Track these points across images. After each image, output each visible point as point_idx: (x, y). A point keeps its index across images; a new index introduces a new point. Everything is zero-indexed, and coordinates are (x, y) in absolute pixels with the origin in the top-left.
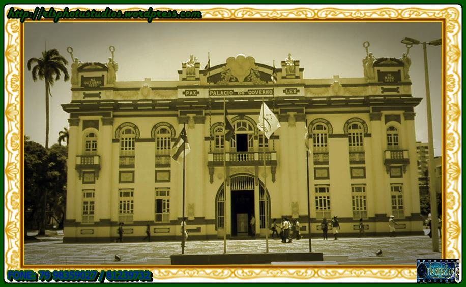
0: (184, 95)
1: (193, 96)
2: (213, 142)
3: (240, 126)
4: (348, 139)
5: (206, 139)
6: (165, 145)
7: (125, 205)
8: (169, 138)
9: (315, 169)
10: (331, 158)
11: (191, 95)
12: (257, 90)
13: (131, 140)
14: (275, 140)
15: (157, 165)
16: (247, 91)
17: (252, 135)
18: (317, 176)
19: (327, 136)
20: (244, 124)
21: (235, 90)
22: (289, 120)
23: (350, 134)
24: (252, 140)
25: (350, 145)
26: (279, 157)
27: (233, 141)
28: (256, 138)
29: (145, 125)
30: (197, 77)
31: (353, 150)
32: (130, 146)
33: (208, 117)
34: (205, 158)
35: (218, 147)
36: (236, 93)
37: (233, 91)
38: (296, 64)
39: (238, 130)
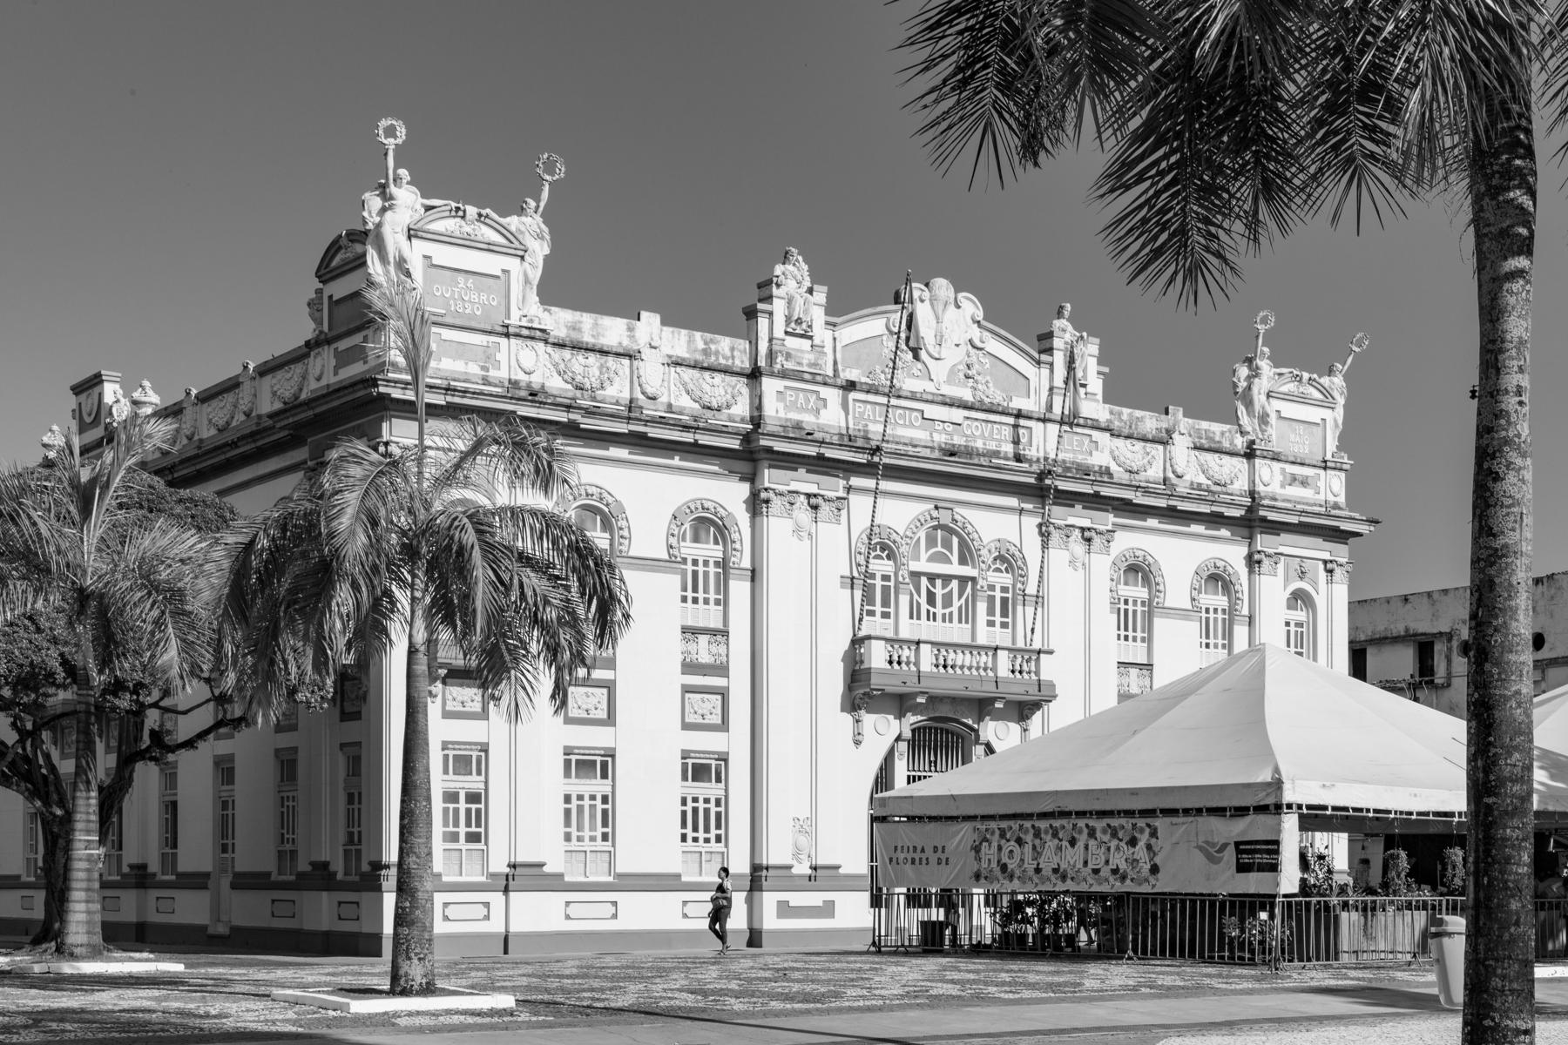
0: (781, 406)
1: (806, 410)
7: (580, 809)
15: (689, 667)
21: (932, 411)
39: (930, 559)
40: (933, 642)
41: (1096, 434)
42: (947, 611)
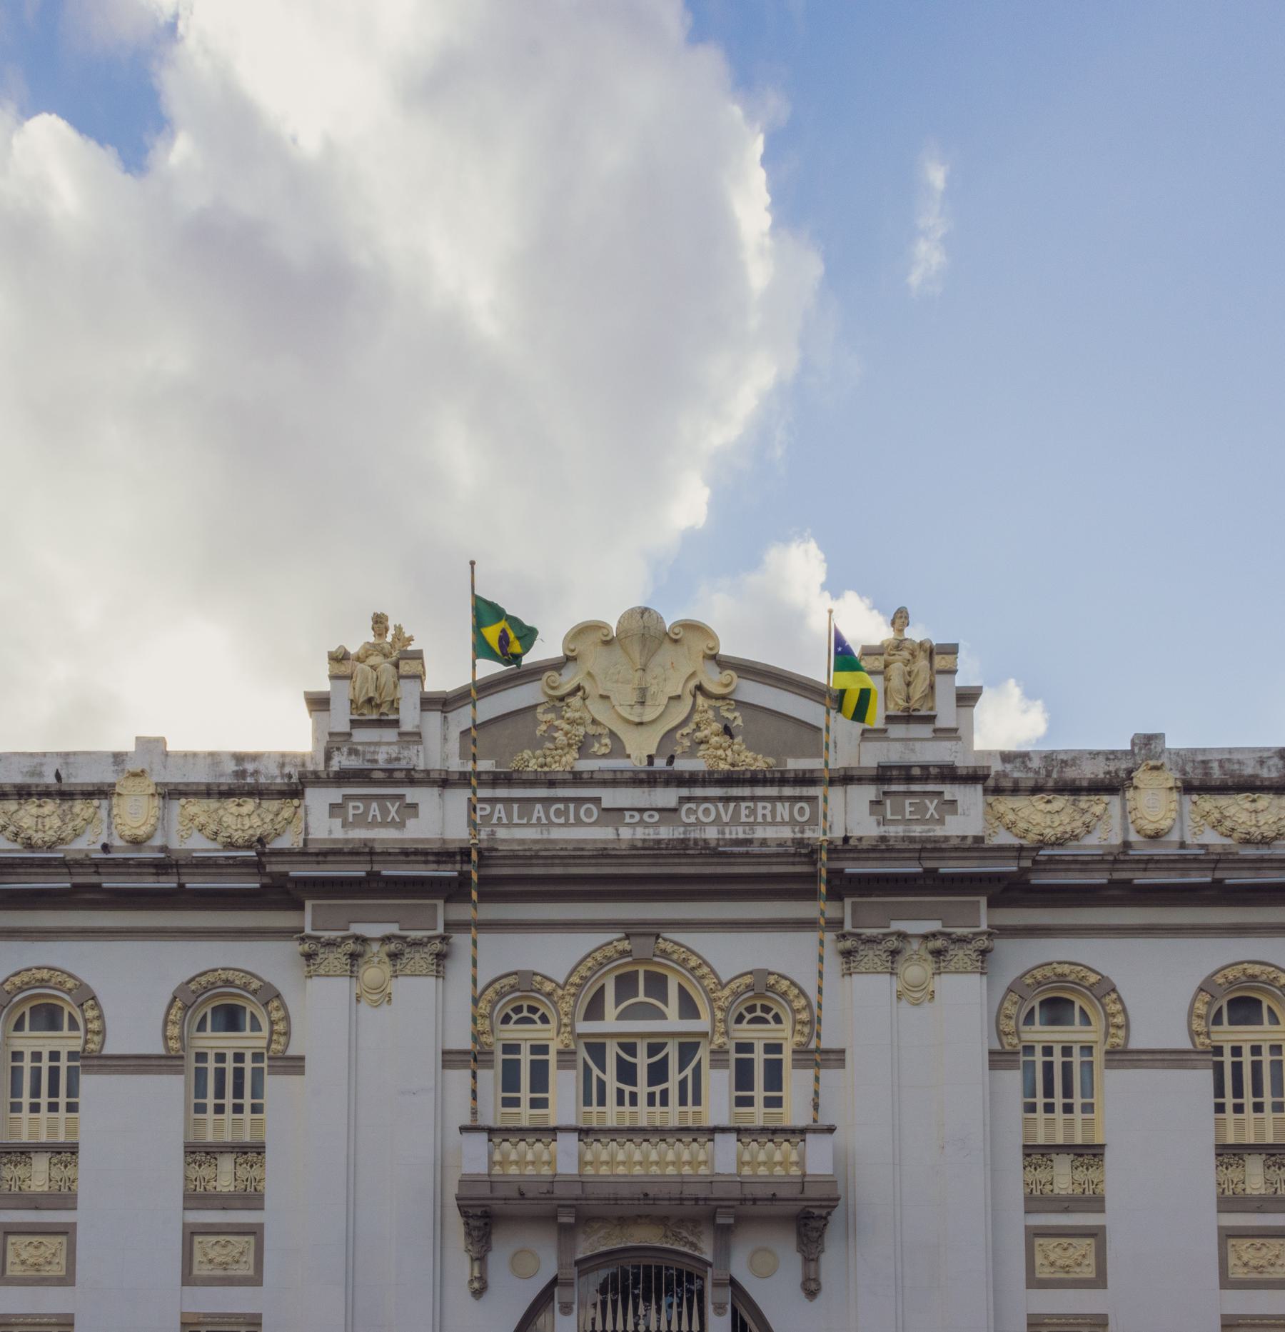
1: (384, 824)
2: (490, 1079)
3: (636, 995)
4: (1208, 1075)
5: (450, 1059)
6: (238, 1092)
8: (257, 1057)
9: (1034, 1233)
10: (1115, 1178)
11: (374, 824)
12: (727, 799)
13: (63, 1064)
14: (823, 1073)
16: (673, 803)
17: (697, 1045)
18: (1043, 1273)
19: (1098, 1057)
20: (657, 984)
21: (610, 797)
22: (900, 969)
23: (1218, 1051)
24: (697, 1071)
25: (1220, 1108)
26: (842, 1159)
27: (596, 1071)
28: (718, 1057)
29: (133, 981)
30: (407, 726)
31: (1231, 1140)
32: (54, 1091)
33: (461, 941)
34: (441, 1166)
35: (515, 1102)
36: (614, 814)
37: (597, 801)
38: (940, 662)
39: (620, 1017)
40: (584, 1140)
41: (950, 791)
42: (657, 1089)
